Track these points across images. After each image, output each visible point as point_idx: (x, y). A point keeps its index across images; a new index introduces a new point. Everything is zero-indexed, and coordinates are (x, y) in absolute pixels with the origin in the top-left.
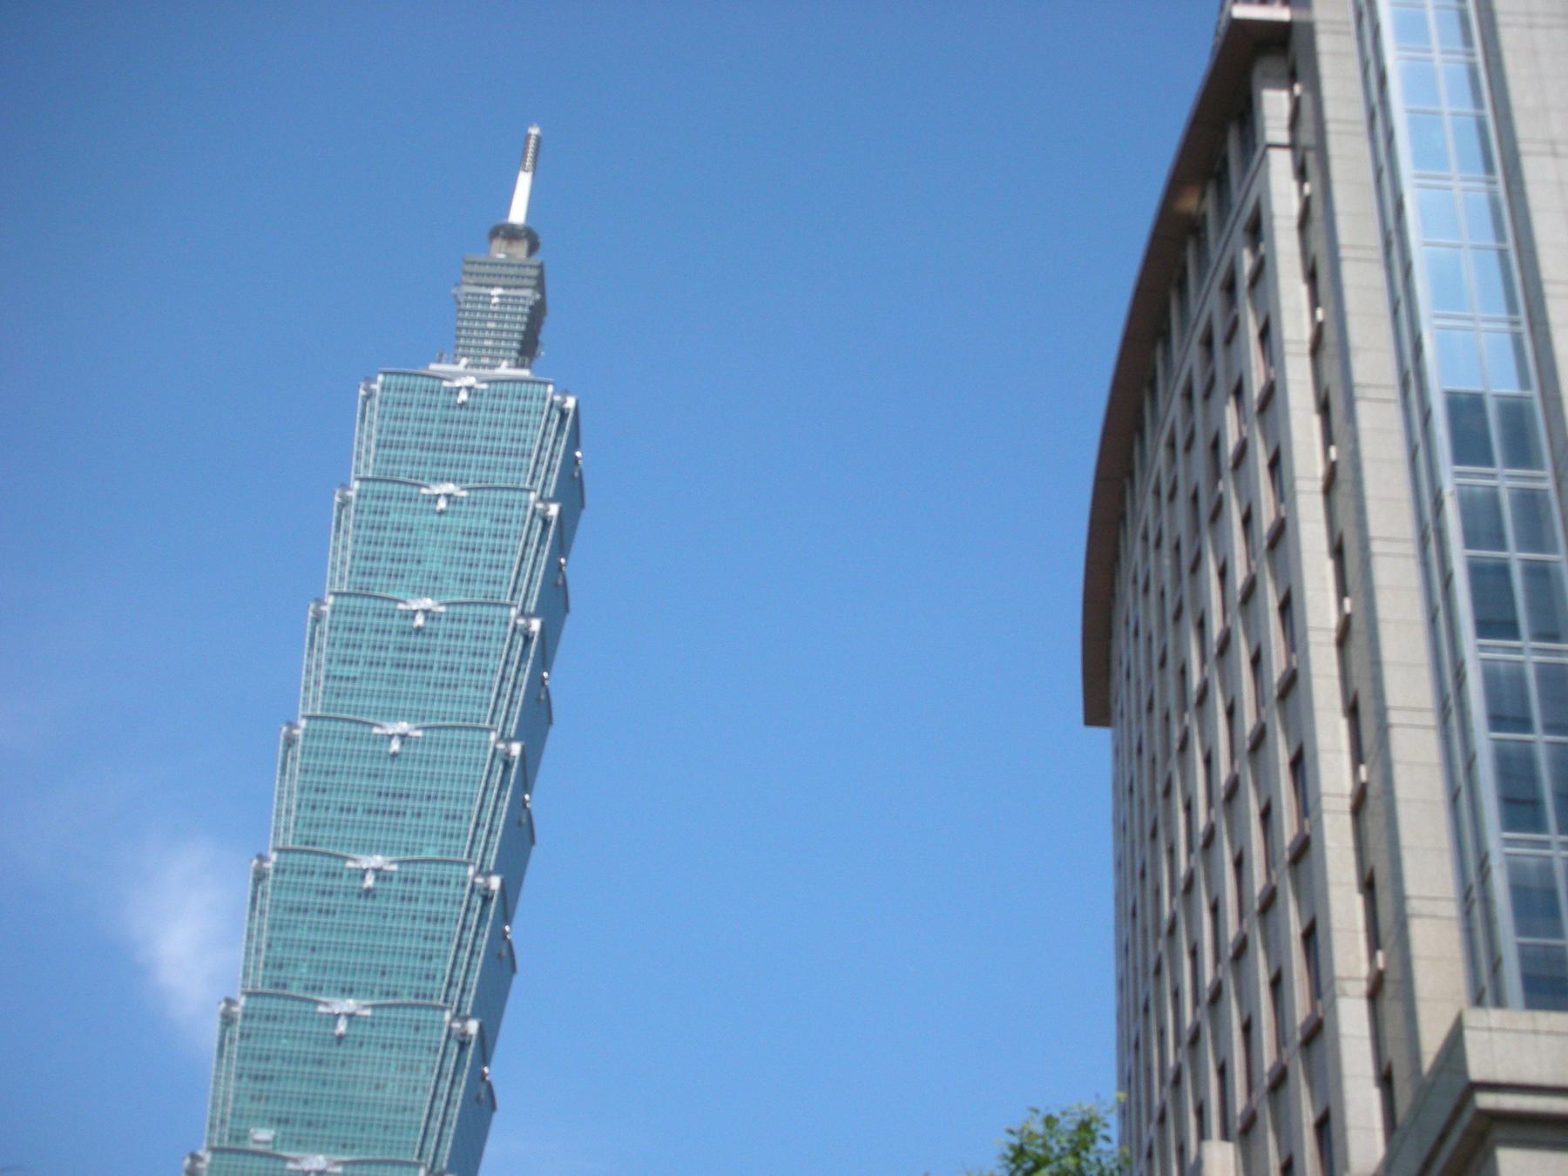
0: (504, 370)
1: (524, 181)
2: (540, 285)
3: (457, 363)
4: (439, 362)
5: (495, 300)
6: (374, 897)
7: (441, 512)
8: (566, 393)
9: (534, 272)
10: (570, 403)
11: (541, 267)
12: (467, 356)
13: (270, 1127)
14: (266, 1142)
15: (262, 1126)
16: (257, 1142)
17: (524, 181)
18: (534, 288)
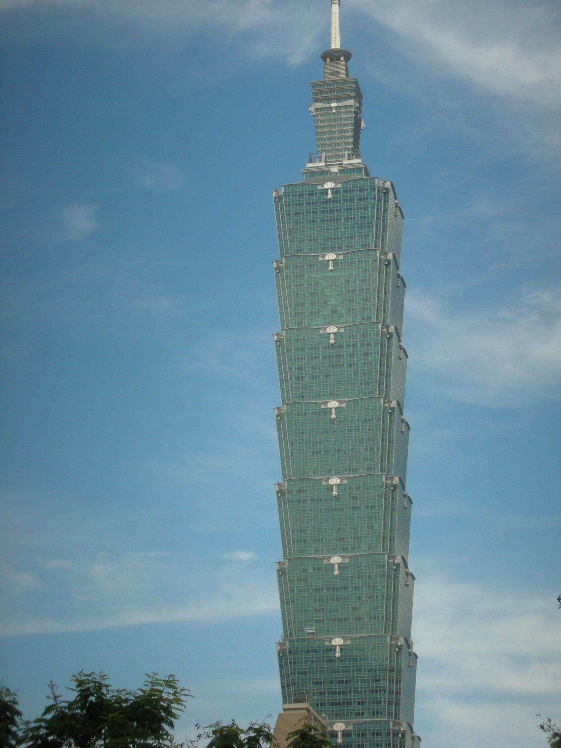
0: (346, 162)
1: (335, 8)
2: (358, 96)
3: (320, 157)
4: (311, 163)
5: (334, 111)
6: (339, 499)
7: (331, 271)
8: (385, 182)
9: (353, 86)
10: (388, 185)
11: (356, 82)
12: (325, 151)
13: (313, 625)
14: (313, 634)
15: (309, 625)
16: (308, 634)
17: (335, 8)
18: (354, 98)
